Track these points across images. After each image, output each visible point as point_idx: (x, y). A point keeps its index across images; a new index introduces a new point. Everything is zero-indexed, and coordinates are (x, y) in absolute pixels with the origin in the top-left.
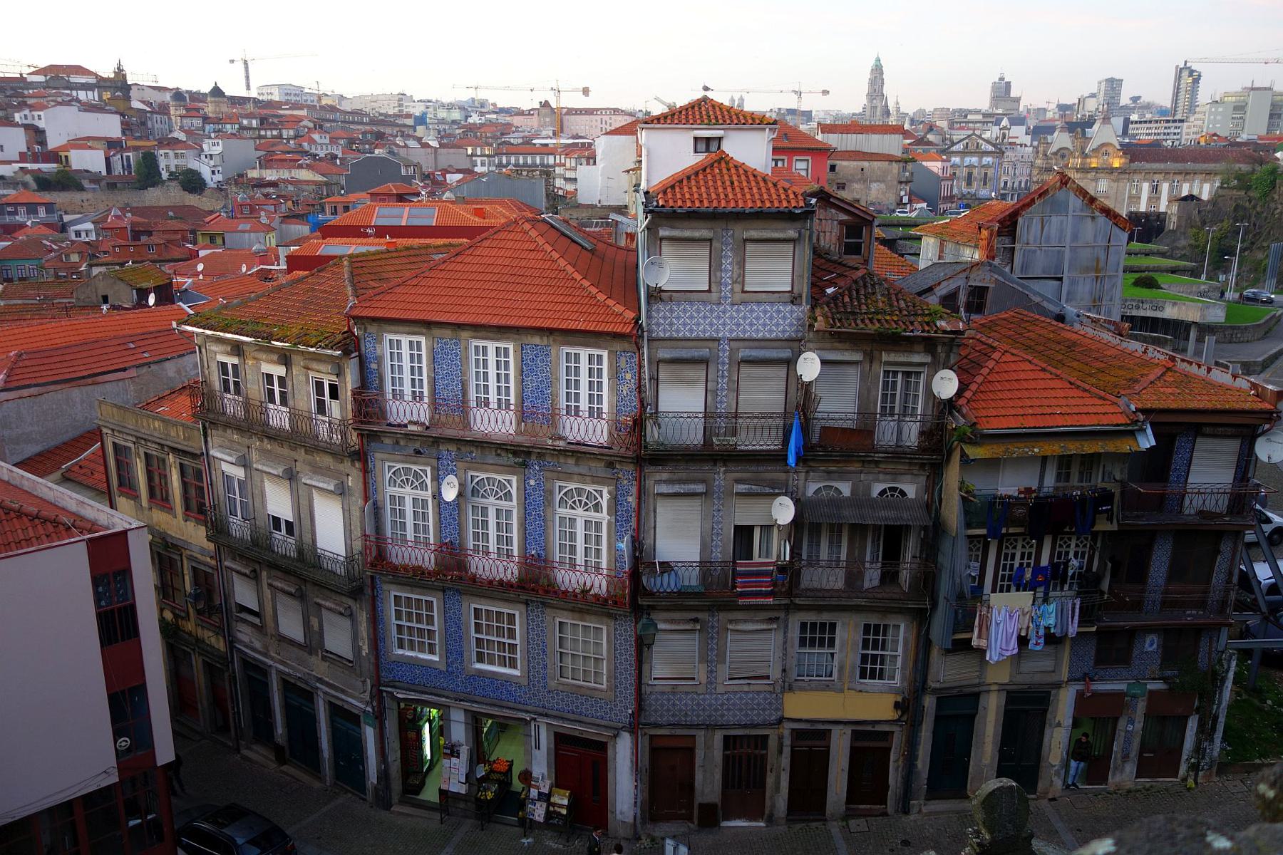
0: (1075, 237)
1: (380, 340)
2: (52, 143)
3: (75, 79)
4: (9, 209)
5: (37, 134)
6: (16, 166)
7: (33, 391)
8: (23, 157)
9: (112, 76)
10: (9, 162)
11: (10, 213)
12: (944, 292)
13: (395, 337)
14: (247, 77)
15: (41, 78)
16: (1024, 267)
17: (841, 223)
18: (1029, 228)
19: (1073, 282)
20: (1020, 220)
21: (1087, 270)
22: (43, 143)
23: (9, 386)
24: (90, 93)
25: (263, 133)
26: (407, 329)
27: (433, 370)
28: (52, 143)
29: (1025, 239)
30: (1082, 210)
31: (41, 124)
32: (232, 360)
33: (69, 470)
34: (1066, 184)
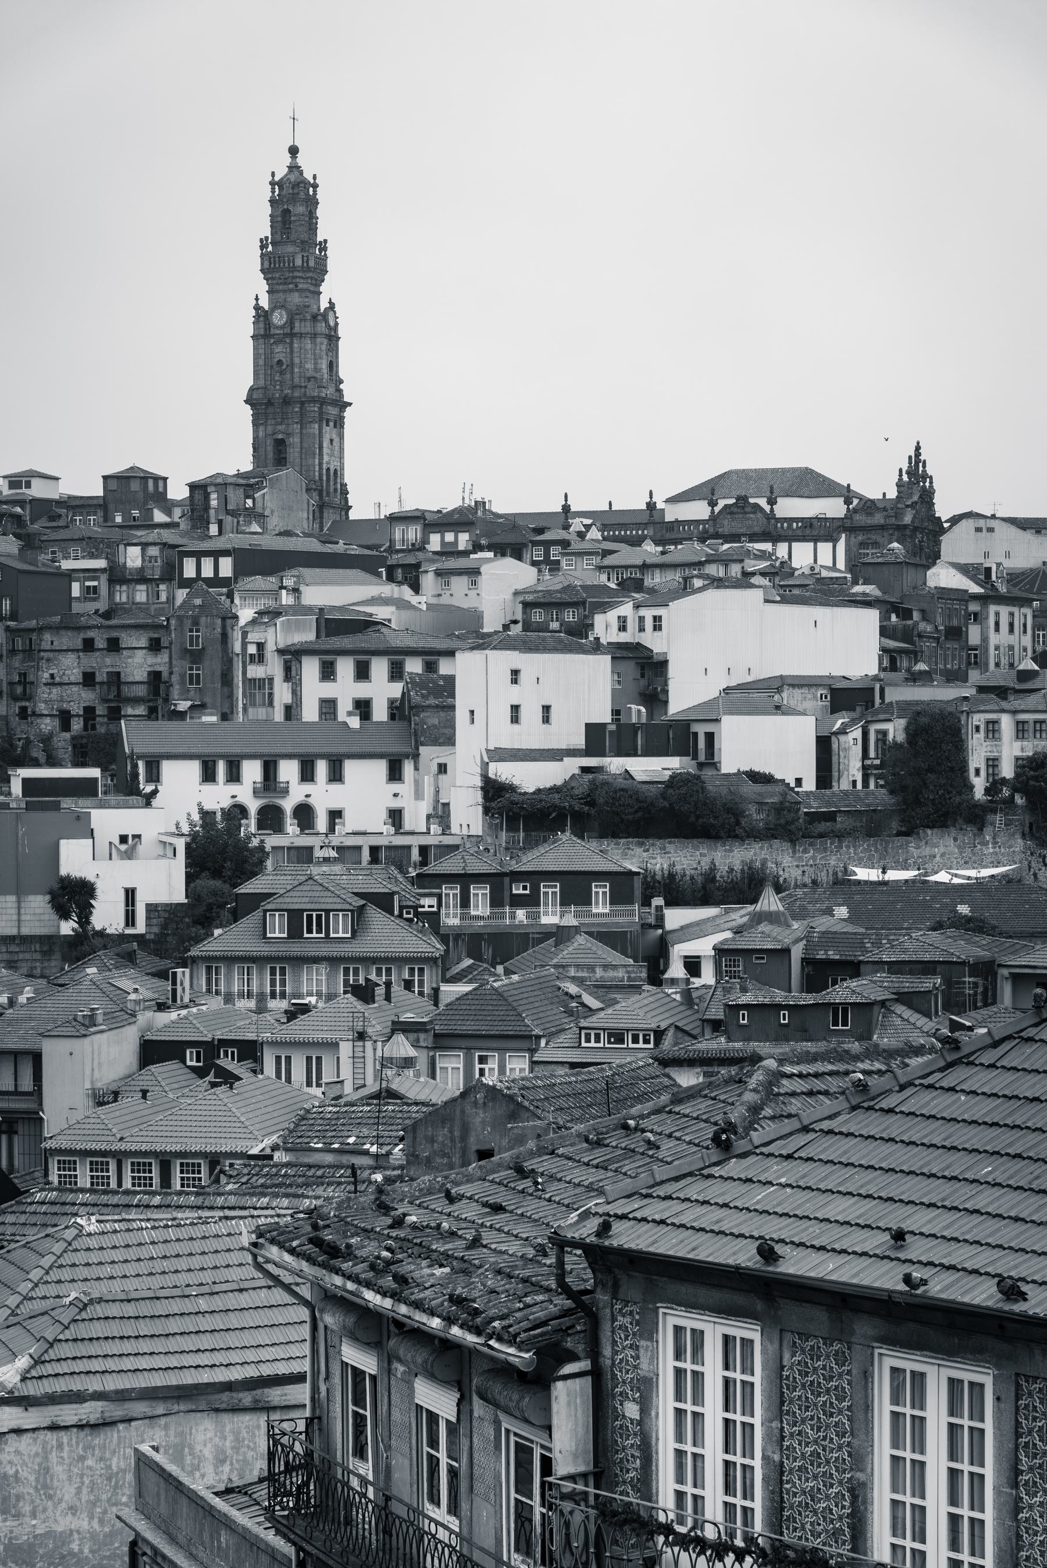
1: (648, 1330)
3: (790, 508)
4: (518, 890)
5: (644, 671)
6: (572, 766)
7: (90, 1411)
8: (596, 738)
9: (892, 494)
11: (518, 902)
13: (690, 1321)
15: (699, 511)
22: (655, 697)
23: (33, 1389)
24: (825, 549)
26: (716, 1296)
27: (778, 1439)
32: (368, 1363)
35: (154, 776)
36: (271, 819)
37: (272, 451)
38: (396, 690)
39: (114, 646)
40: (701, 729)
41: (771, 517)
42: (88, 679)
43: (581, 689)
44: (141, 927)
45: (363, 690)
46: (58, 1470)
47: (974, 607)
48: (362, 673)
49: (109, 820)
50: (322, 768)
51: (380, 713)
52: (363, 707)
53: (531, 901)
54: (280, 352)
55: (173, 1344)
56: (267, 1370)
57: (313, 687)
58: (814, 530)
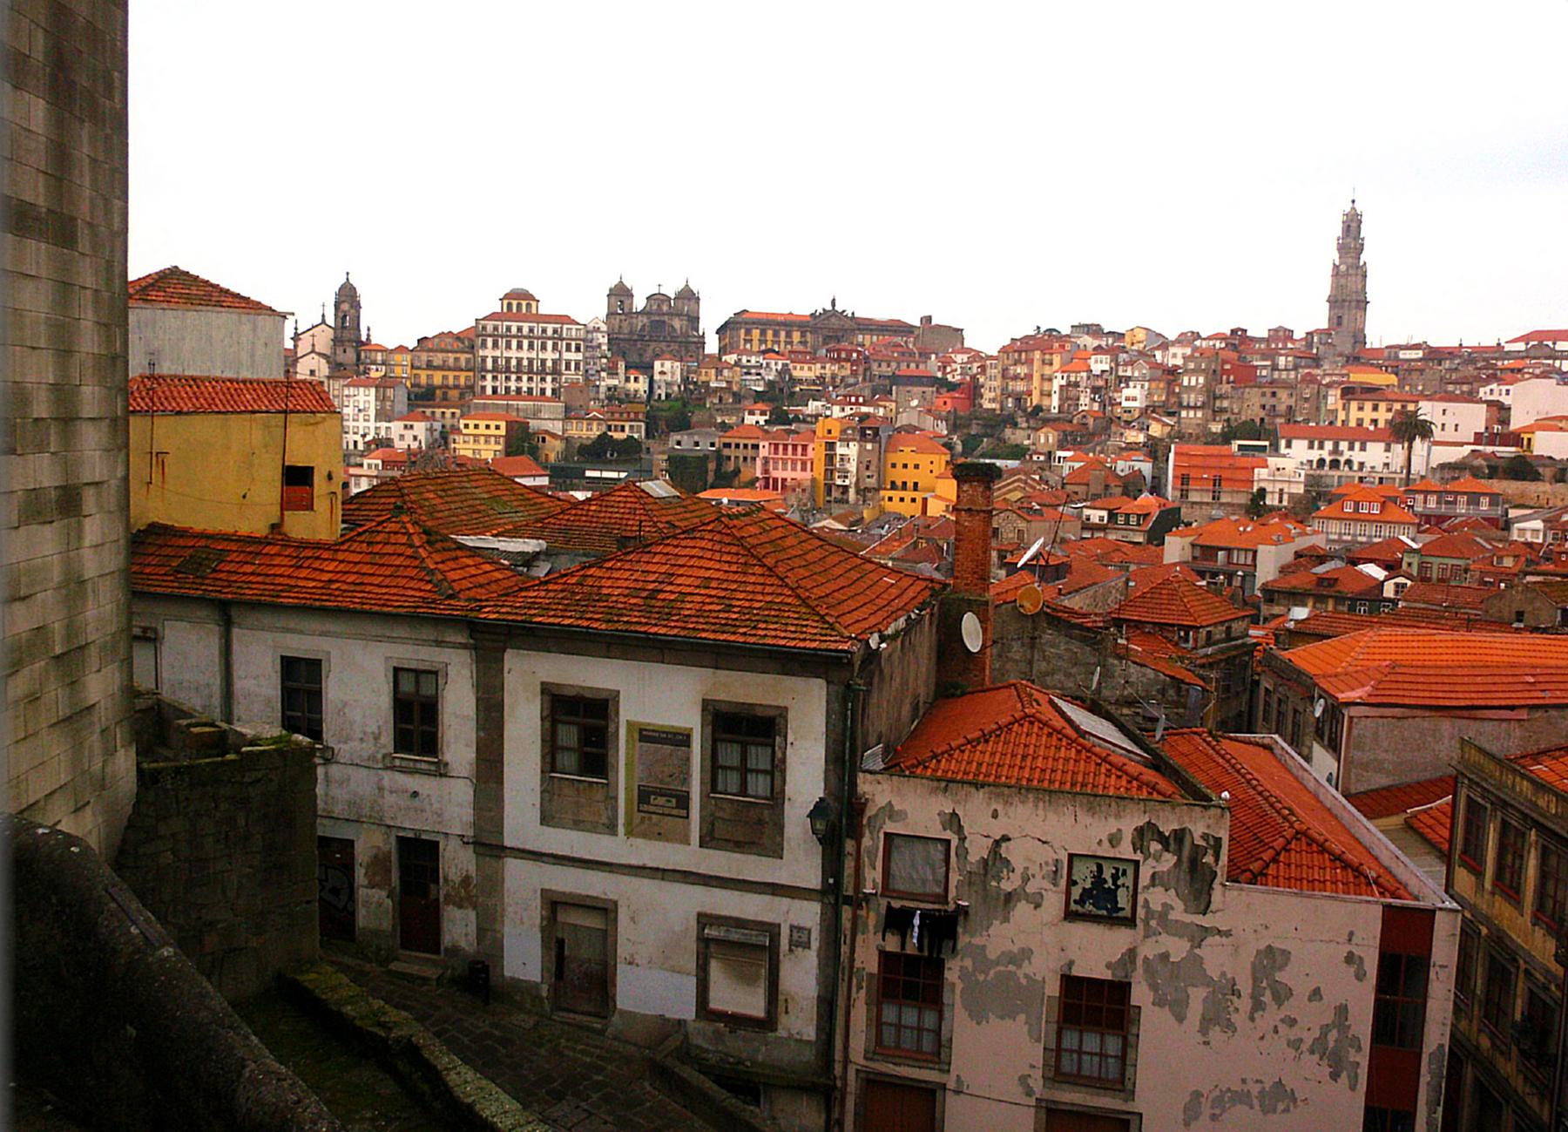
2: (1515, 425)
5: (1501, 412)
6: (1467, 449)
7: (1398, 711)
8: (1478, 439)
10: (1462, 444)
15: (1521, 346)
22: (1505, 422)
23: (1373, 700)
28: (1513, 426)
31: (1506, 400)
33: (1414, 816)
35: (1289, 446)
36: (1335, 464)
37: (1337, 321)
38: (1390, 416)
39: (1274, 394)
40: (1525, 436)
42: (1263, 407)
43: (1473, 418)
44: (1285, 503)
45: (1375, 415)
46: (1382, 734)
48: (1375, 408)
49: (1272, 461)
50: (1357, 445)
51: (1381, 425)
52: (1375, 422)
53: (1455, 502)
54: (1343, 281)
55: (1434, 687)
56: (1476, 703)
57: (1354, 414)
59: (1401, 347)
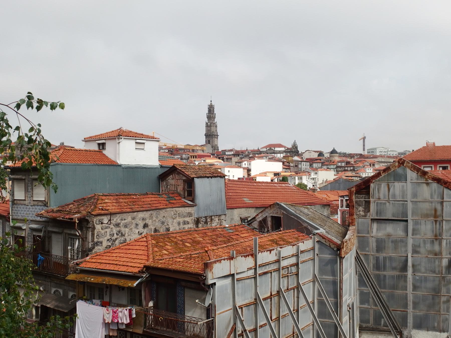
0: (415, 195)
2: (253, 174)
3: (277, 149)
12: (261, 219)
14: (364, 145)
15: (265, 150)
16: (378, 212)
17: (184, 181)
18: (379, 191)
19: (416, 223)
20: (372, 185)
21: (427, 216)
22: (249, 175)
25: (346, 168)
29: (376, 195)
30: (417, 179)
34: (403, 163)
37: (208, 142)
40: (254, 179)
41: (274, 150)
47: (300, 162)
58: (280, 152)
59: (225, 151)
